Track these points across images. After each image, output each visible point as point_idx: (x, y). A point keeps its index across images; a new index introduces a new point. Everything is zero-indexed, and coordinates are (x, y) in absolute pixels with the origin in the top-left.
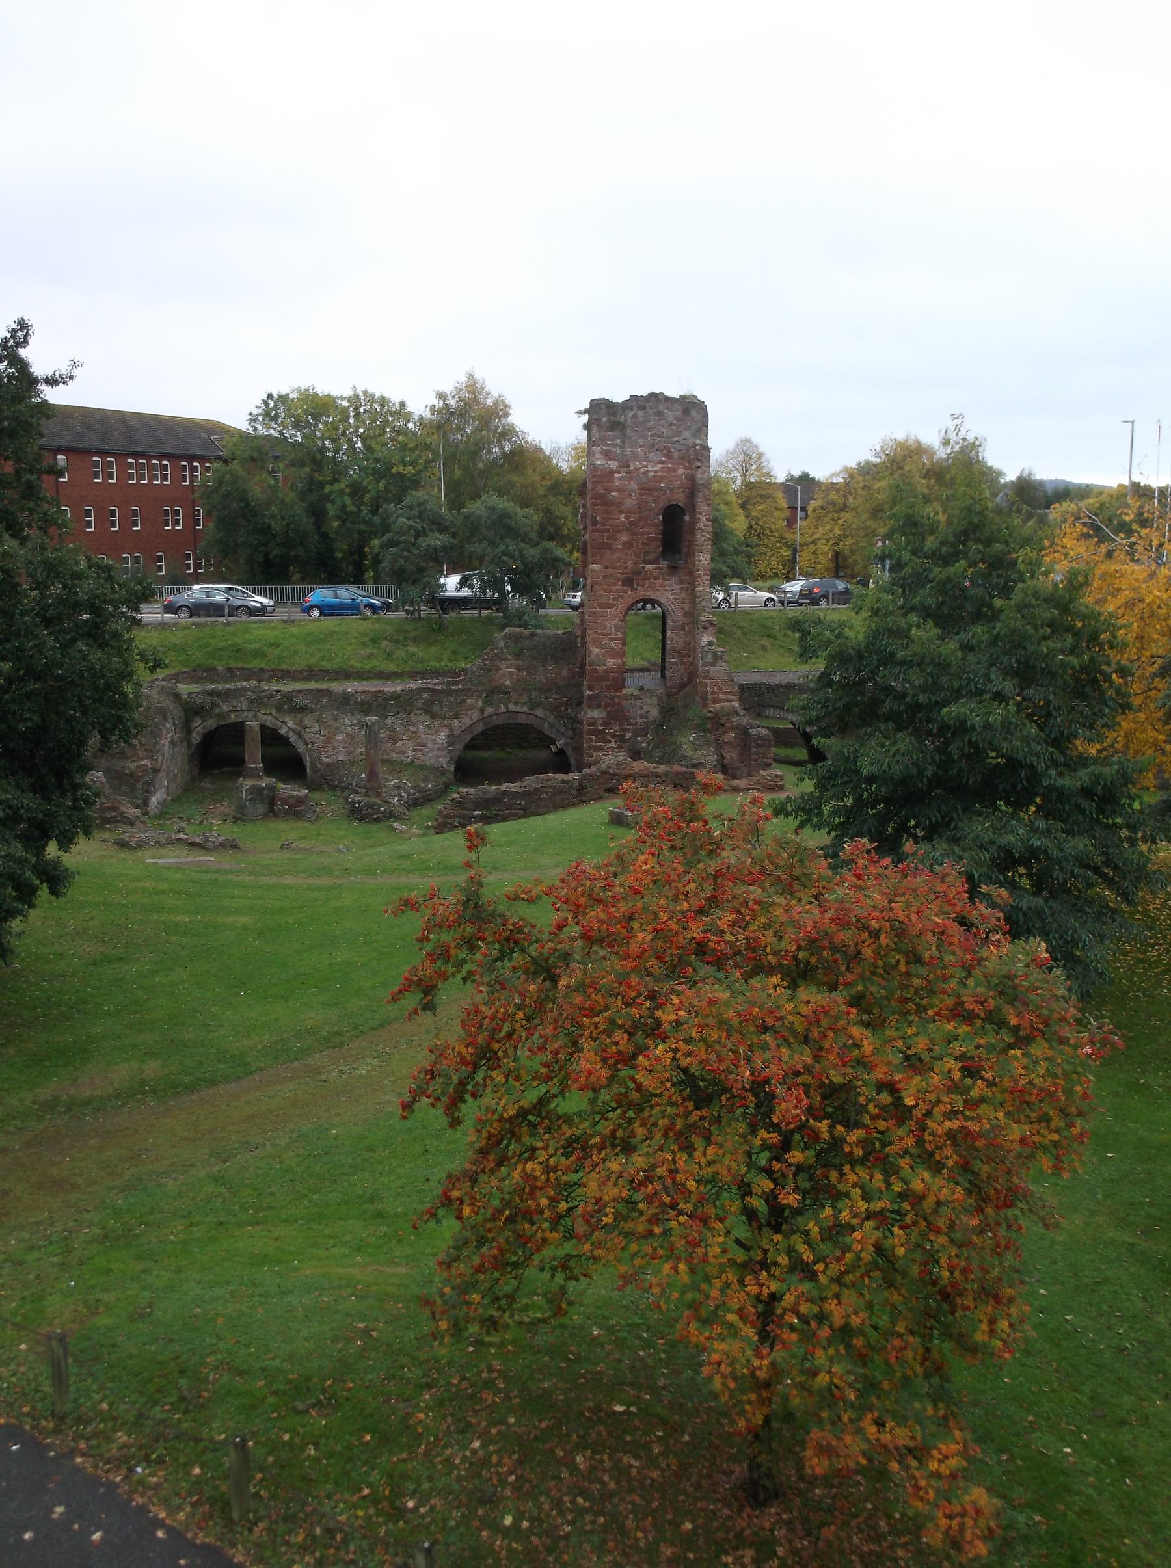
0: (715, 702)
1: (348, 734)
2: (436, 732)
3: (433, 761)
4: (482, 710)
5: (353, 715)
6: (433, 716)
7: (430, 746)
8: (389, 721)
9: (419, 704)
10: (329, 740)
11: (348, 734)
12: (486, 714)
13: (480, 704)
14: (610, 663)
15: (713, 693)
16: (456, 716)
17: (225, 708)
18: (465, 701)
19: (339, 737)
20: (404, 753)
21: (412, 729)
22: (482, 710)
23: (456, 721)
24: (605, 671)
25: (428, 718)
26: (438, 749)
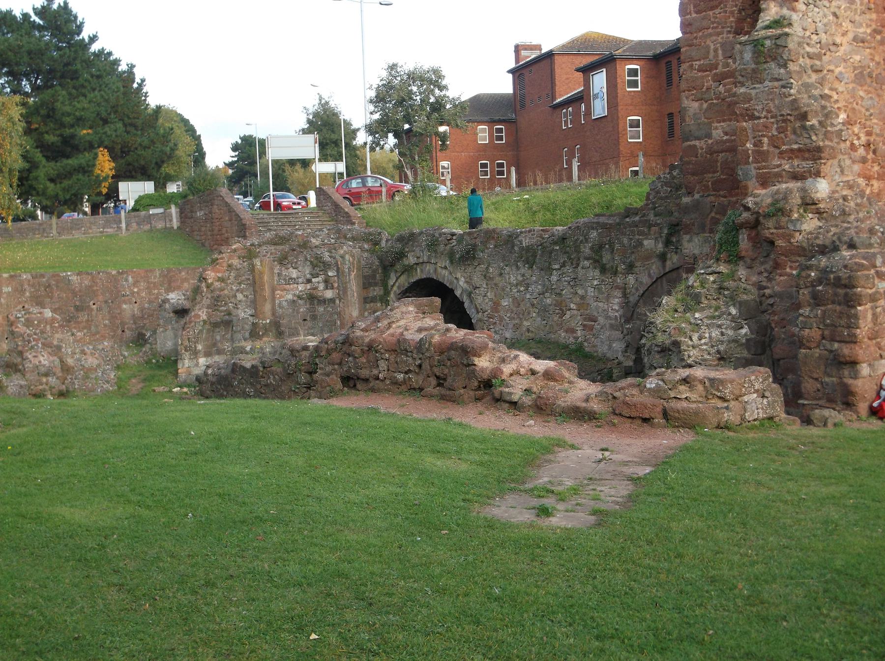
0: (765, 181)
1: (515, 299)
2: (608, 298)
3: (605, 348)
4: (663, 257)
5: (518, 268)
6: (603, 270)
7: (601, 320)
8: (554, 278)
9: (586, 250)
10: (496, 306)
11: (515, 299)
12: (669, 265)
13: (660, 247)
14: (718, 132)
15: (761, 156)
16: (630, 268)
17: (411, 260)
18: (640, 244)
19: (505, 303)
20: (572, 331)
21: (580, 292)
22: (663, 257)
23: (631, 279)
24: (711, 151)
25: (597, 273)
26: (612, 327)
